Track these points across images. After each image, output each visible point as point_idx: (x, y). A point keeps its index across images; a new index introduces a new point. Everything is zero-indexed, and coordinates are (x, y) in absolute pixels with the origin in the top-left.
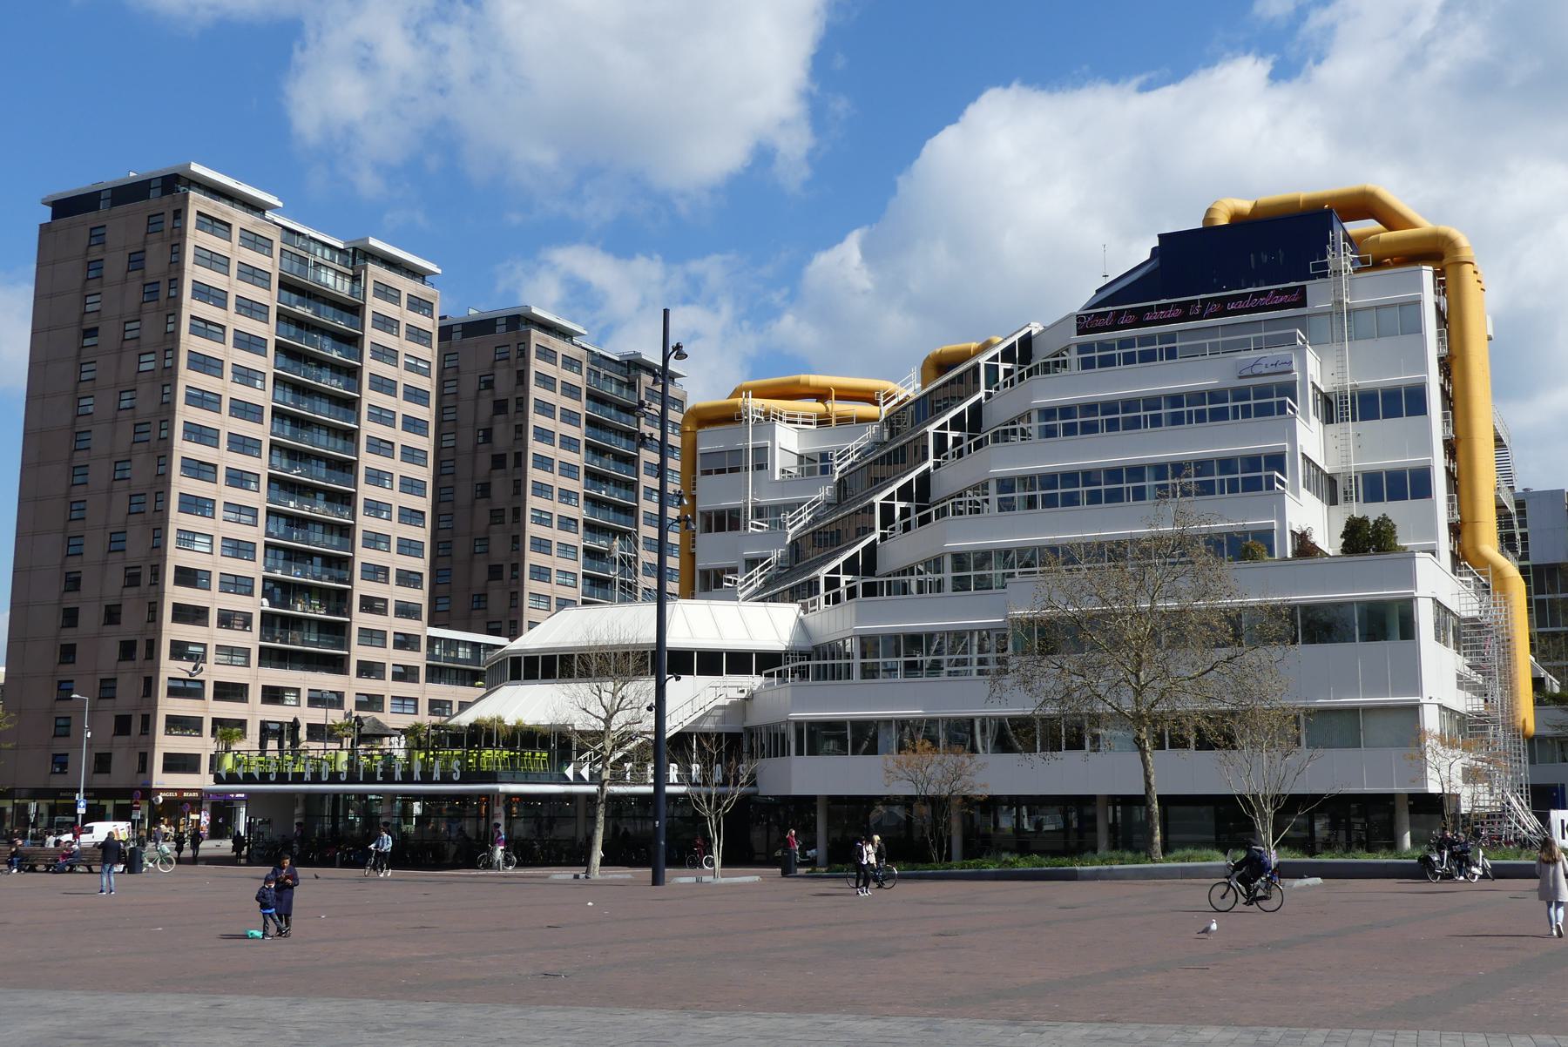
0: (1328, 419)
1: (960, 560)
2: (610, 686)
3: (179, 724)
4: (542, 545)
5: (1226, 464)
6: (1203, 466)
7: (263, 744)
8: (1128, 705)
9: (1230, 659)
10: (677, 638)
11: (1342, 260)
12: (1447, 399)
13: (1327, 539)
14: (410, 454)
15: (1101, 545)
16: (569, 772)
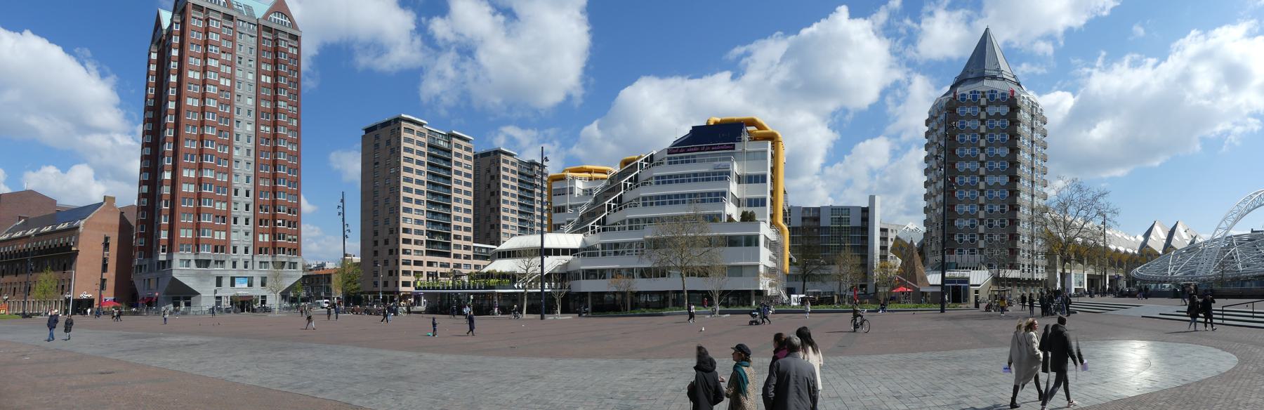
0: (739, 183)
1: (631, 221)
2: (527, 260)
3: (406, 273)
4: (506, 218)
5: (709, 194)
6: (703, 194)
7: (428, 278)
8: (679, 264)
10: (546, 245)
11: (745, 137)
12: (772, 179)
13: (736, 217)
14: (467, 193)
15: (672, 217)
16: (516, 286)
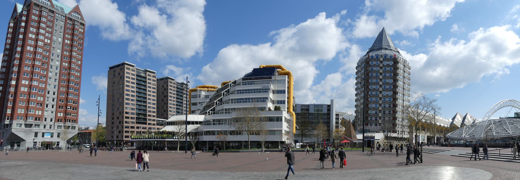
0: (273, 93)
1: (226, 109)
2: (180, 126)
3: (126, 132)
4: (171, 107)
5: (260, 98)
6: (258, 98)
7: (137, 134)
8: (247, 129)
9: (260, 123)
10: (188, 120)
11: (276, 74)
12: (288, 92)
13: (272, 108)
14: (153, 96)
15: (244, 108)
16: (174, 138)
